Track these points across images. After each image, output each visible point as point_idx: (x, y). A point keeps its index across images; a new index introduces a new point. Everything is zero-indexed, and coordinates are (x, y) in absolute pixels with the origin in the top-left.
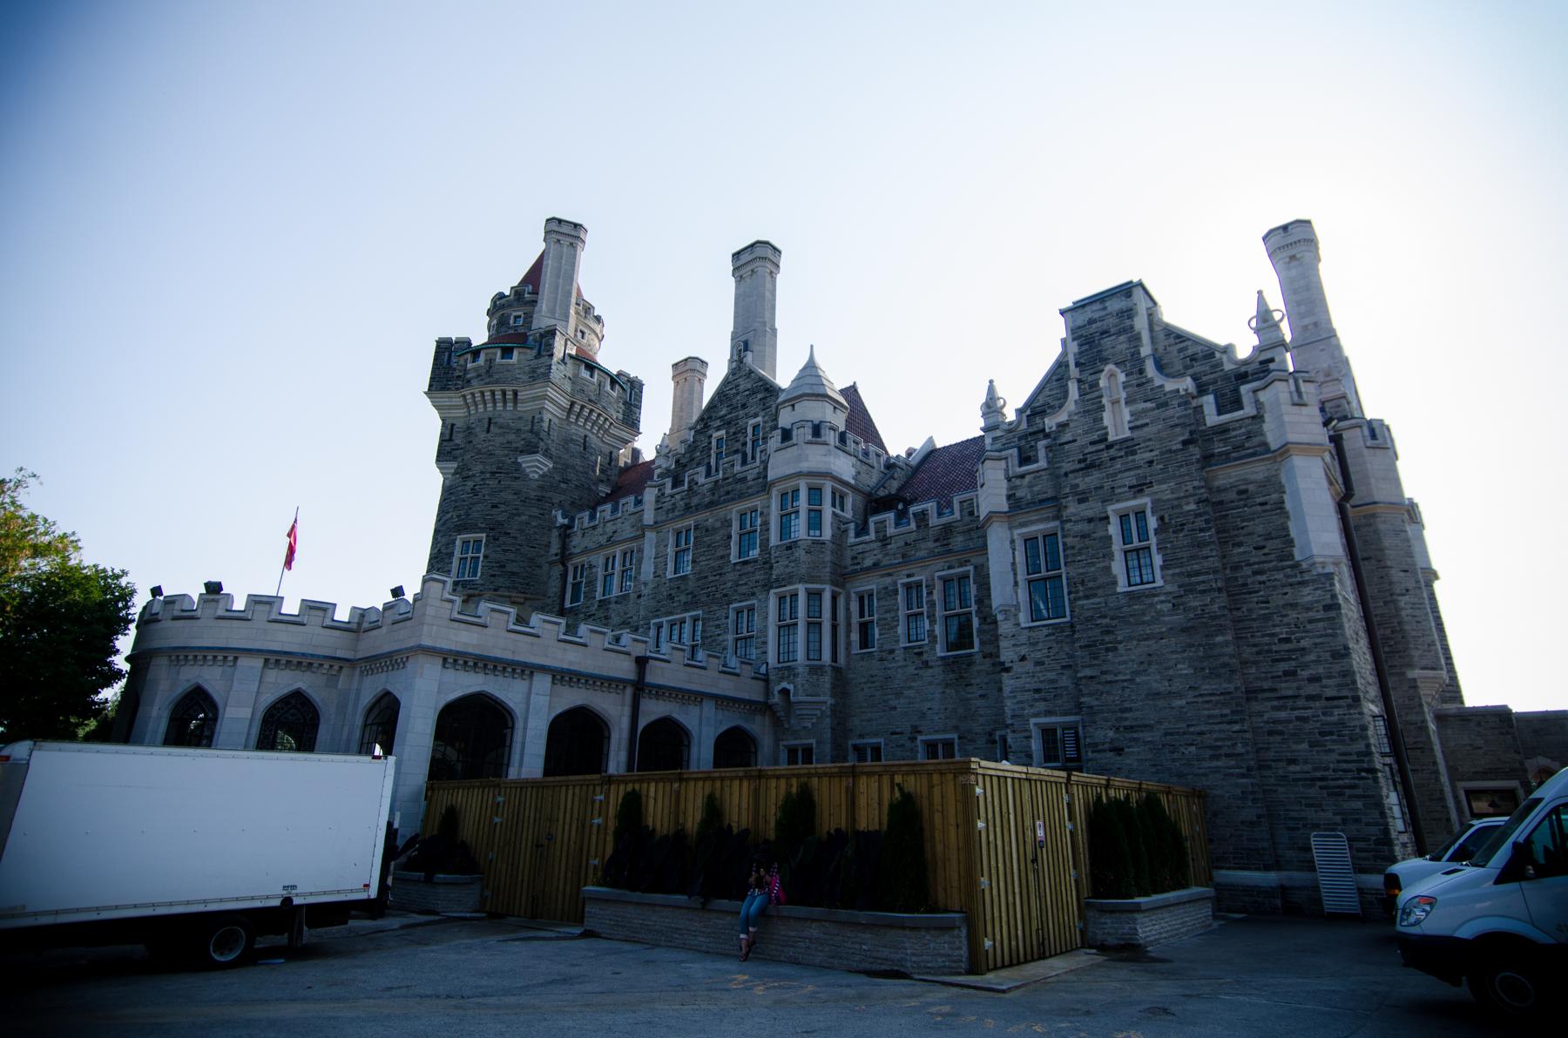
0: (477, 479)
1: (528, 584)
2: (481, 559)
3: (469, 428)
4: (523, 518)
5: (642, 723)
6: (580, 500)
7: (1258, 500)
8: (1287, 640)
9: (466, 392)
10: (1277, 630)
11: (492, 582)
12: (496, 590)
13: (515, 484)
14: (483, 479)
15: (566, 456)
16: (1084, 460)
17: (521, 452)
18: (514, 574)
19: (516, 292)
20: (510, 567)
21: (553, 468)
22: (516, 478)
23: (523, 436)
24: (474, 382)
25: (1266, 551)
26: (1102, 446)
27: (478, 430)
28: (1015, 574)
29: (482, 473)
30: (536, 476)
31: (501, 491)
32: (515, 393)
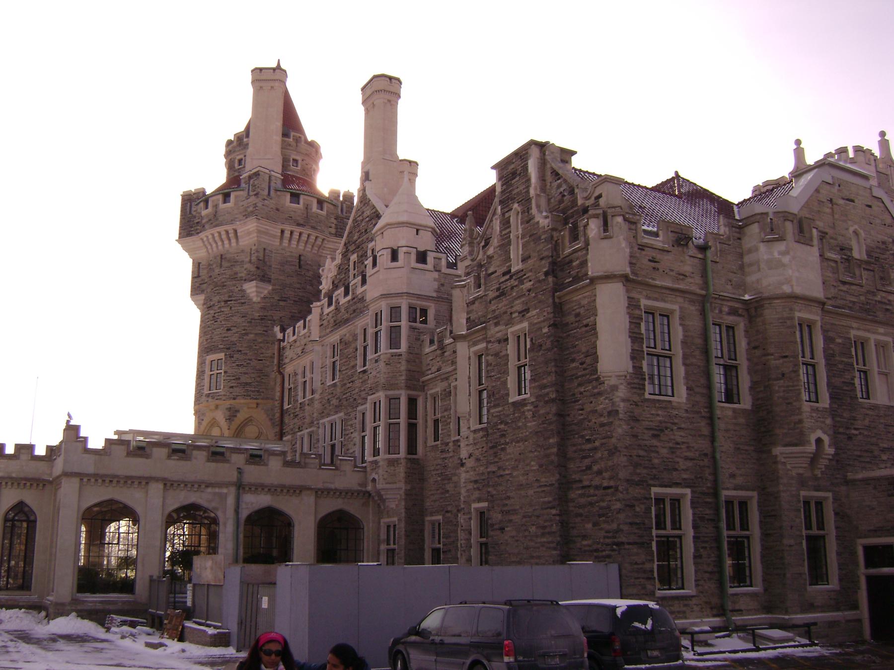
0: (216, 308)
1: (258, 391)
2: (223, 374)
3: (210, 265)
4: (251, 336)
5: (244, 514)
6: (299, 313)
7: (585, 322)
8: (589, 441)
9: (202, 235)
10: (585, 432)
11: (231, 393)
12: (234, 399)
13: (242, 309)
14: (220, 308)
15: (282, 278)
16: (500, 287)
17: (245, 280)
18: (247, 384)
19: (238, 137)
20: (244, 379)
21: (273, 290)
22: (243, 303)
23: (245, 266)
24: (207, 226)
25: (584, 366)
26: (507, 277)
27: (214, 266)
28: (470, 386)
29: (219, 302)
30: (259, 299)
31: (232, 316)
32: (235, 231)
